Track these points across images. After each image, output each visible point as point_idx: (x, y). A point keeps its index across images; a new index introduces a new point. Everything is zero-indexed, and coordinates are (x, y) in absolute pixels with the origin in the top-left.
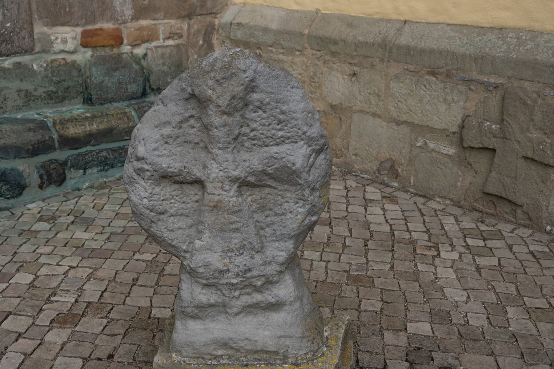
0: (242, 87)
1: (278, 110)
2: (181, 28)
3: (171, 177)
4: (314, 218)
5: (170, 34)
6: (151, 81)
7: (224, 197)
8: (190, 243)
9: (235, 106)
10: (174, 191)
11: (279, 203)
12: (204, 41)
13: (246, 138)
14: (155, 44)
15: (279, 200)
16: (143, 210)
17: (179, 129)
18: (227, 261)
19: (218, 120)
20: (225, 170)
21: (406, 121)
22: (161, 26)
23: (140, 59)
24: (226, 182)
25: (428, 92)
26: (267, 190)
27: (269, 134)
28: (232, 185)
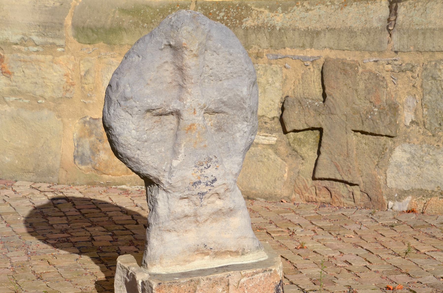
3: (154, 110)
10: (155, 122)
16: (131, 140)
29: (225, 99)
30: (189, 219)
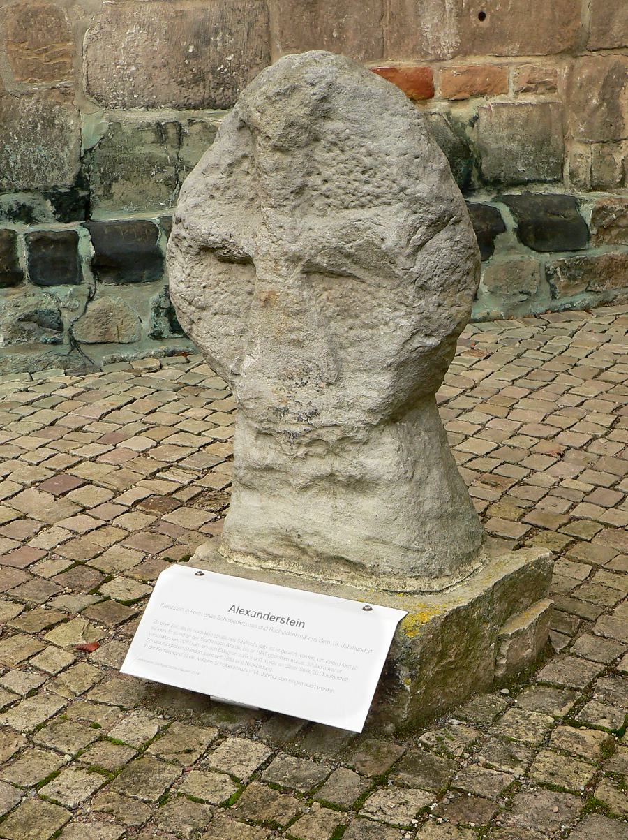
0: (306, 109)
1: (363, 150)
2: (555, 74)
5: (528, 83)
6: (483, 166)
7: (279, 286)
9: (294, 138)
10: (220, 274)
11: (367, 305)
12: (602, 99)
13: (315, 193)
14: (497, 100)
15: (368, 301)
16: (180, 301)
17: (229, 176)
18: (284, 393)
19: (268, 159)
20: (279, 242)
22: (512, 68)
23: (463, 125)
24: (282, 263)
26: (350, 283)
27: (350, 188)
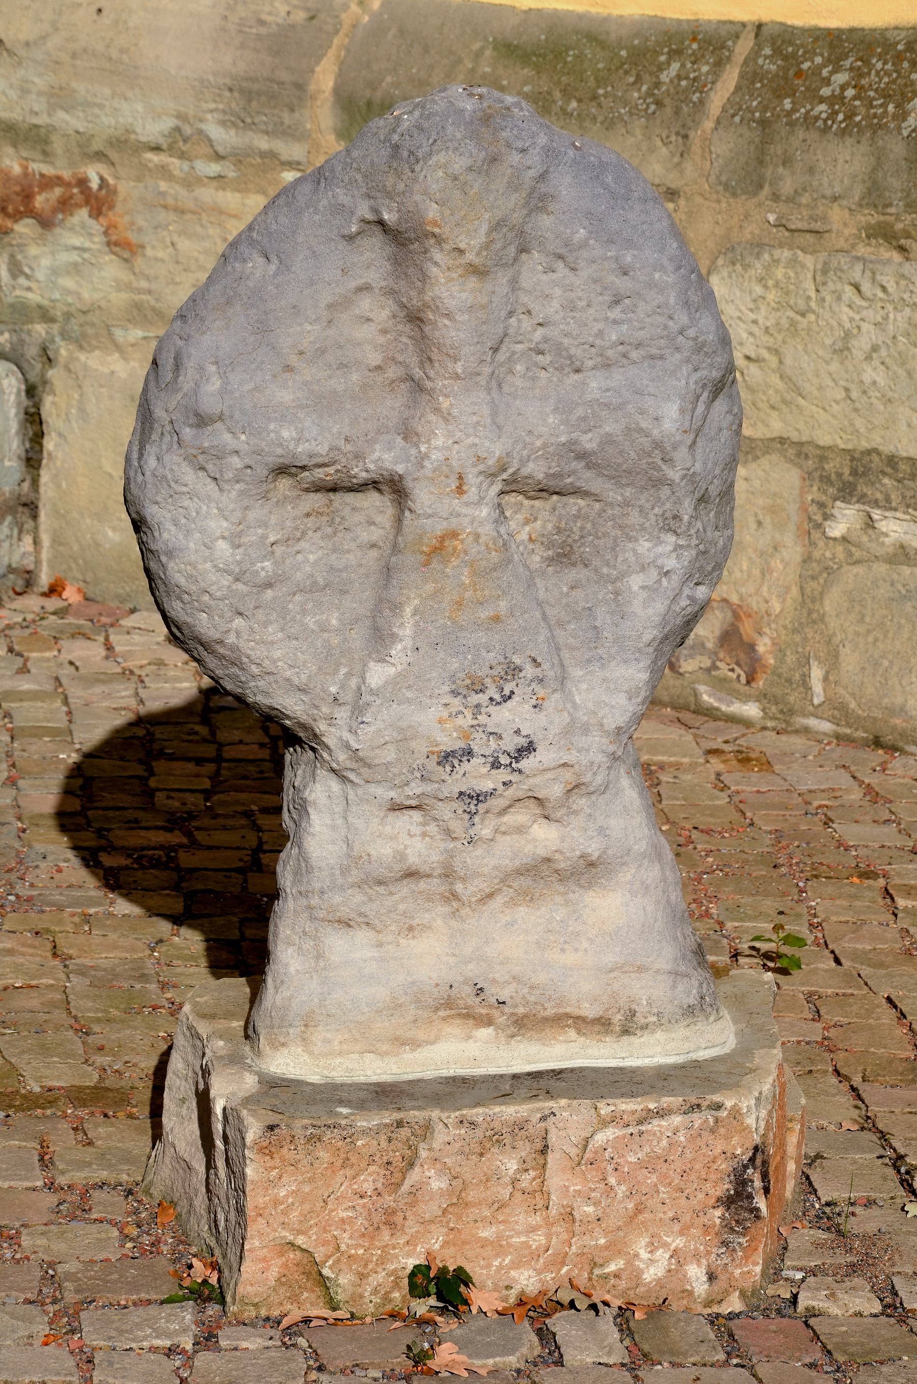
3: (304, 468)
4: (701, 592)
8: (349, 675)
10: (308, 515)
13: (520, 347)
21: (782, 440)
25: (869, 314)
26: (575, 504)
28: (484, 487)
29: (589, 442)
30: (423, 885)
